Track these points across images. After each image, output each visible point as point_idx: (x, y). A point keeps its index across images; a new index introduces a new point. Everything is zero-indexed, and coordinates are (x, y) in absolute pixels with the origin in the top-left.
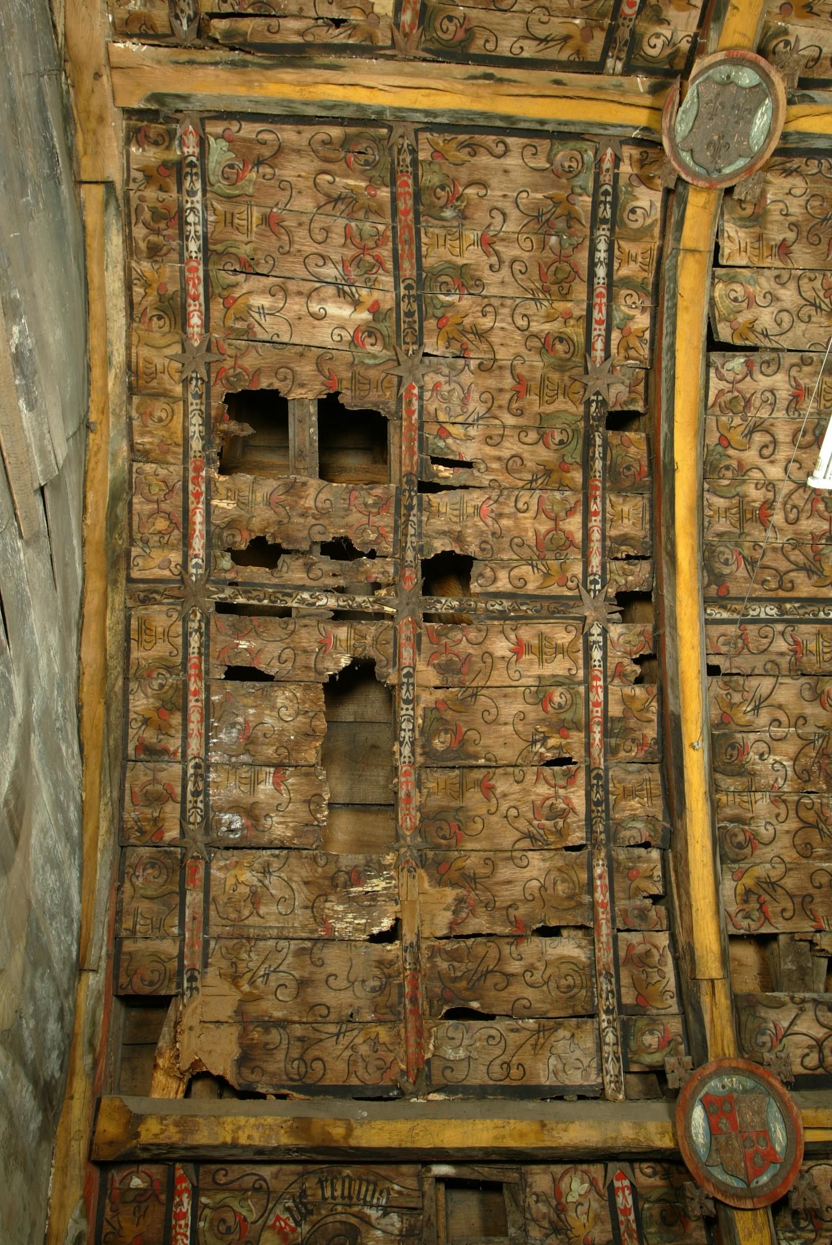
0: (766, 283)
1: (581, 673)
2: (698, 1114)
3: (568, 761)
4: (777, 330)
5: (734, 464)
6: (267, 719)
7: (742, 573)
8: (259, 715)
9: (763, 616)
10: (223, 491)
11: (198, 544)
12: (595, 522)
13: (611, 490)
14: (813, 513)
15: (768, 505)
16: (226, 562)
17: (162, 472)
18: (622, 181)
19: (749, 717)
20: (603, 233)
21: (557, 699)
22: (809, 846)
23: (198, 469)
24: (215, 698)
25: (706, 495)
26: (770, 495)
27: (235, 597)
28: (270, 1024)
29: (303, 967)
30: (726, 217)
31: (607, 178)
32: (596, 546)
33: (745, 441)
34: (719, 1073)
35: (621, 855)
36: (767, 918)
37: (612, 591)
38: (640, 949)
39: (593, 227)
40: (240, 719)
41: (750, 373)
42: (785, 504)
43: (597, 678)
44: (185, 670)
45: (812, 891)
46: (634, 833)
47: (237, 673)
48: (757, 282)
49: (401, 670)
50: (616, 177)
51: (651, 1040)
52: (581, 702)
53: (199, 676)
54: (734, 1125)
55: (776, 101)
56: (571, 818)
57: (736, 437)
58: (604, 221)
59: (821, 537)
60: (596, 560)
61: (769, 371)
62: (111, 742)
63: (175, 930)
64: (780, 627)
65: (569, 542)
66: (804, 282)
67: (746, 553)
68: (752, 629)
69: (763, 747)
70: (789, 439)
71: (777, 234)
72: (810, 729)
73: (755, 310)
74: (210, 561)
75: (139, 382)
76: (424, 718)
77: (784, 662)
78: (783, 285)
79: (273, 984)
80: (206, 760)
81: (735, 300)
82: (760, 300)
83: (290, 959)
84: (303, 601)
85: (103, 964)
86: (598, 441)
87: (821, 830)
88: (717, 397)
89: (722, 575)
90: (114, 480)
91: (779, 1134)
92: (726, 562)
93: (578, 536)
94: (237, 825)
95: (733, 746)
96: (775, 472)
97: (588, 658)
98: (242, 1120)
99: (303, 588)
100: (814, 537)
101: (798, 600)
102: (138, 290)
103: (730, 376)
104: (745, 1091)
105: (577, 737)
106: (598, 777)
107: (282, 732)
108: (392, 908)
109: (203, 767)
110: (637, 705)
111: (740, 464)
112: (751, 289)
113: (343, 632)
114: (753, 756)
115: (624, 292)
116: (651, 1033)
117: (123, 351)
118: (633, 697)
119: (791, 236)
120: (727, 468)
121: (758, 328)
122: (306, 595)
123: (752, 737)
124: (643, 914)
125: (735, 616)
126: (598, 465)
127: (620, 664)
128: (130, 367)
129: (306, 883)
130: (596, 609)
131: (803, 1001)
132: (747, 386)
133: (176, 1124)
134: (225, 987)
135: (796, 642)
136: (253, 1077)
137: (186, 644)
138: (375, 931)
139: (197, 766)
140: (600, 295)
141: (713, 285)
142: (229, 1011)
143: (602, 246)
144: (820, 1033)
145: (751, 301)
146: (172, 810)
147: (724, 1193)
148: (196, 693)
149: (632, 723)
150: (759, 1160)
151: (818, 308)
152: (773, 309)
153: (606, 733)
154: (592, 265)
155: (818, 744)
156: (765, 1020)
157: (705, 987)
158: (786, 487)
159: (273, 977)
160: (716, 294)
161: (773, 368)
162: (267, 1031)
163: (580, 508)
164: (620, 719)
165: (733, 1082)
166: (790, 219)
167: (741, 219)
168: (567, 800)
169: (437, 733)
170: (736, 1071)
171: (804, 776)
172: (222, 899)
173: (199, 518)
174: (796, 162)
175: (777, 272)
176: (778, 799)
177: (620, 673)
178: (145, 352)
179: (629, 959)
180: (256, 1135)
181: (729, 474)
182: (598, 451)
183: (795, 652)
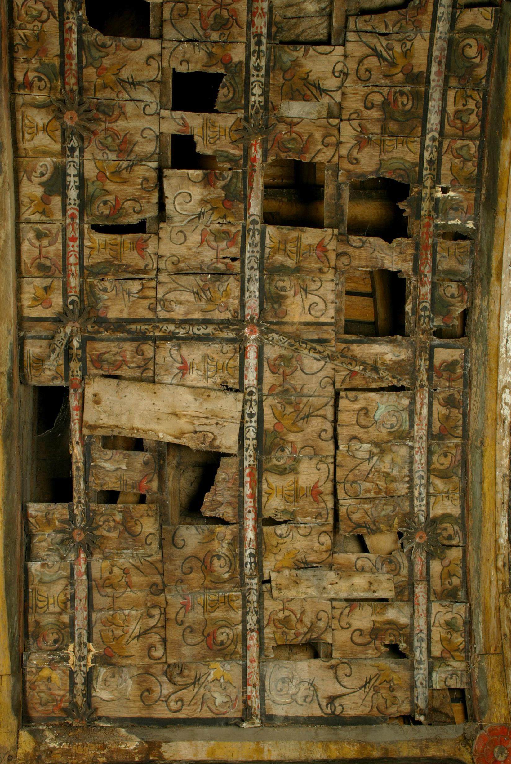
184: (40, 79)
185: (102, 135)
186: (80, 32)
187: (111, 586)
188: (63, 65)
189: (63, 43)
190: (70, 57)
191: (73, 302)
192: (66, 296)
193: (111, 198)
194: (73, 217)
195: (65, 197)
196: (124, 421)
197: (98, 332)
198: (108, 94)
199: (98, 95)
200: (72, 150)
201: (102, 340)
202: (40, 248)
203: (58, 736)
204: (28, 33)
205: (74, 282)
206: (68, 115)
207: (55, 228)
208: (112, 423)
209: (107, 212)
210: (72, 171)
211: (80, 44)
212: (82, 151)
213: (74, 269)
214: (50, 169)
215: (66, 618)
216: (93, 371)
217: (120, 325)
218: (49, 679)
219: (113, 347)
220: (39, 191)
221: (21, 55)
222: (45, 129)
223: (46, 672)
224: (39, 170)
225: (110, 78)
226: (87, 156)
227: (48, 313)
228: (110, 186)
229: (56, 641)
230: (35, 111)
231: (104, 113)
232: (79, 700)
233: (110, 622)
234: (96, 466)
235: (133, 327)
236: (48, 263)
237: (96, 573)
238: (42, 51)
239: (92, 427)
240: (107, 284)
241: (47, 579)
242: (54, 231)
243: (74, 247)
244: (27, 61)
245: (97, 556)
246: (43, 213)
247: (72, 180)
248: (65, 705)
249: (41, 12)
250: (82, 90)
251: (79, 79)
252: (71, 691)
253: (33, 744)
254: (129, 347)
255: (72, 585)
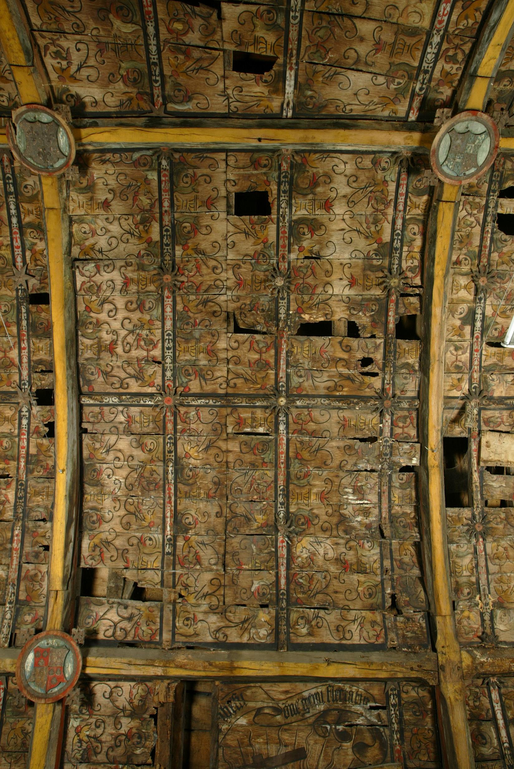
0: (101, 223)
1: (16, 431)
2: (31, 657)
3: (7, 476)
4: (109, 248)
5: (95, 321)
7: (101, 379)
9: (111, 402)
12: (25, 353)
13: (33, 336)
14: (138, 346)
15: (114, 343)
18: (17, 171)
19: (104, 455)
20: (12, 199)
21: (5, 444)
22: (129, 523)
25: (80, 338)
26: (115, 337)
30: (71, 188)
31: (8, 170)
32: (25, 365)
33: (100, 308)
34: (46, 637)
35: (30, 524)
36: (102, 560)
37: (34, 389)
38: (32, 573)
39: (7, 197)
41: (98, 271)
42: (123, 342)
43: (24, 434)
45: (128, 547)
46: (38, 513)
48: (96, 223)
50: (13, 169)
51: (28, 618)
52: (16, 446)
54: (46, 663)
55: (65, 129)
56: (7, 505)
57: (94, 306)
58: (11, 193)
59: (142, 360)
60: (25, 373)
61: (109, 270)
64: (120, 408)
65: (12, 364)
66: (122, 221)
67: (103, 368)
68: (106, 409)
69: (109, 472)
70: (124, 307)
71: (102, 196)
72: (135, 462)
73: (96, 237)
77: (121, 427)
78: (111, 223)
81: (85, 233)
82: (99, 232)
86: (24, 310)
87: (136, 516)
88: (82, 285)
89: (90, 381)
91: (69, 669)
92: (92, 374)
93: (17, 361)
95: (95, 471)
96: (116, 325)
97: (20, 424)
100: (138, 360)
101: (129, 394)
103: (87, 274)
104: (58, 647)
105: (13, 464)
106: (22, 485)
110: (44, 448)
111: (98, 321)
112: (93, 226)
114: (104, 476)
115: (29, 230)
116: (29, 614)
118: (42, 445)
119: (110, 197)
120: (91, 323)
121: (97, 247)
123: (105, 466)
124: (37, 555)
125: (97, 402)
126: (24, 323)
127: (37, 427)
130: (24, 398)
131: (113, 603)
132: (98, 279)
135: (129, 417)
140: (16, 233)
141: (71, 225)
143: (12, 207)
144: (116, 619)
145: (94, 233)
147: (32, 695)
149: (42, 457)
150: (54, 681)
151: (132, 235)
152: (107, 237)
153: (27, 462)
154: (10, 217)
155: (138, 471)
156: (92, 611)
157: (53, 594)
158: (123, 333)
160: (74, 230)
161: (111, 268)
163: (17, 346)
164: (35, 455)
165: (53, 642)
166: (109, 187)
167: (80, 189)
168: (6, 496)
170: (56, 636)
171: (130, 487)
174: (108, 156)
175: (106, 217)
176: (116, 499)
177: (37, 431)
179: (26, 577)
181: (91, 326)
182: (24, 316)
183: (128, 422)
184: (466, 259)
185: (498, 291)
186: (493, 233)
187: (498, 558)
188: (480, 251)
189: (482, 239)
190: (485, 247)
191: (475, 388)
192: (471, 383)
193: (499, 326)
194: (477, 338)
195: (473, 326)
196: (503, 457)
197: (489, 405)
198: (504, 267)
199: (499, 268)
200: (480, 299)
201: (490, 409)
202: (457, 356)
203: (483, 655)
204: (463, 233)
205: (476, 375)
206: (482, 279)
207: (466, 344)
208: (496, 459)
209: (496, 335)
210: (479, 311)
211: (492, 239)
212: (485, 300)
213: (476, 368)
214: (466, 310)
215: (473, 579)
216: (484, 428)
217: (501, 400)
218: (469, 618)
219: (497, 414)
220: (458, 323)
221: (457, 246)
222: (465, 287)
223: (466, 613)
224: (459, 311)
225: (506, 258)
226: (488, 302)
227: (458, 394)
228: (499, 320)
229: (468, 594)
230: (461, 277)
231: (500, 278)
232: (488, 631)
233: (500, 581)
234: (487, 485)
235: (508, 401)
236: (461, 364)
237: (489, 551)
238: (470, 243)
239: (485, 462)
240: (494, 377)
241: (461, 555)
242: (466, 346)
243: (476, 355)
244: (460, 249)
245: (489, 539)
246: (459, 335)
247: (479, 317)
248: (480, 634)
249: (472, 222)
250: (490, 265)
251: (489, 260)
252: (482, 625)
253: (470, 659)
254: (505, 413)
255: (476, 558)
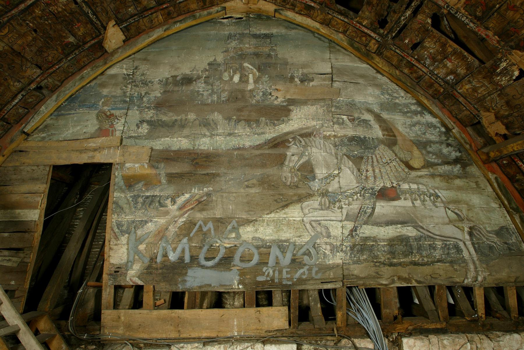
6: (431, 51)
8: (428, 52)
10: (361, 21)
11: (373, 35)
16: (382, 31)
17: (350, 31)
23: (353, 23)
24: (416, 57)
27: (392, 35)
28: (507, 117)
29: (503, 98)
40: (426, 56)
44: (404, 58)
47: (415, 46)
49: (444, 8)
53: (407, 56)
62: (409, 85)
63: (464, 108)
74: (379, 34)
75: (326, 23)
76: (466, 11)
79: (499, 107)
80: (430, 70)
83: (498, 99)
84: (404, 20)
85: (454, 126)
90: (347, 43)
94: (453, 78)
98: (512, 145)
99: (400, 18)
102: (302, 13)
107: (437, 51)
108: (514, 68)
109: (431, 72)
113: (420, 17)
117: (317, 23)
122: (403, 18)
128: (321, 23)
129: (484, 78)
133: (497, 151)
134: (488, 114)
136: (513, 131)
137: (397, 53)
138: (514, 78)
139: (430, 73)
142: (494, 119)
146: (436, 85)
148: (411, 60)
159: (497, 105)
162: (507, 119)
169: (475, 11)
172: (468, 95)
173: (366, 31)
178: (318, 19)
180: (519, 147)
